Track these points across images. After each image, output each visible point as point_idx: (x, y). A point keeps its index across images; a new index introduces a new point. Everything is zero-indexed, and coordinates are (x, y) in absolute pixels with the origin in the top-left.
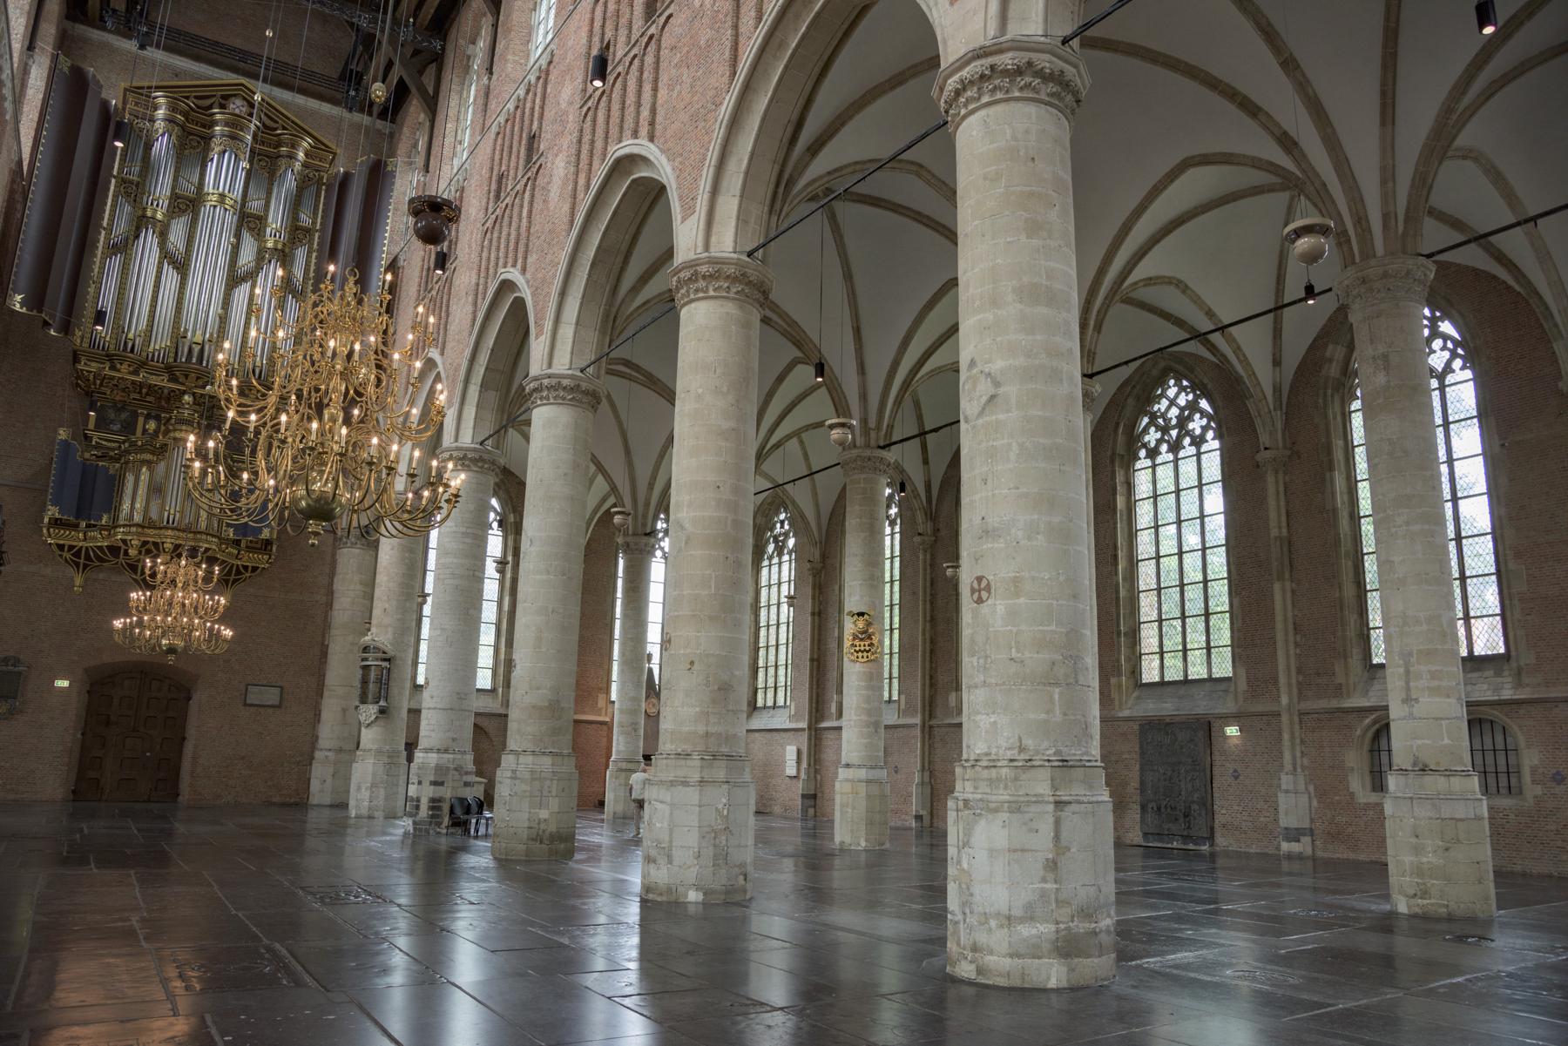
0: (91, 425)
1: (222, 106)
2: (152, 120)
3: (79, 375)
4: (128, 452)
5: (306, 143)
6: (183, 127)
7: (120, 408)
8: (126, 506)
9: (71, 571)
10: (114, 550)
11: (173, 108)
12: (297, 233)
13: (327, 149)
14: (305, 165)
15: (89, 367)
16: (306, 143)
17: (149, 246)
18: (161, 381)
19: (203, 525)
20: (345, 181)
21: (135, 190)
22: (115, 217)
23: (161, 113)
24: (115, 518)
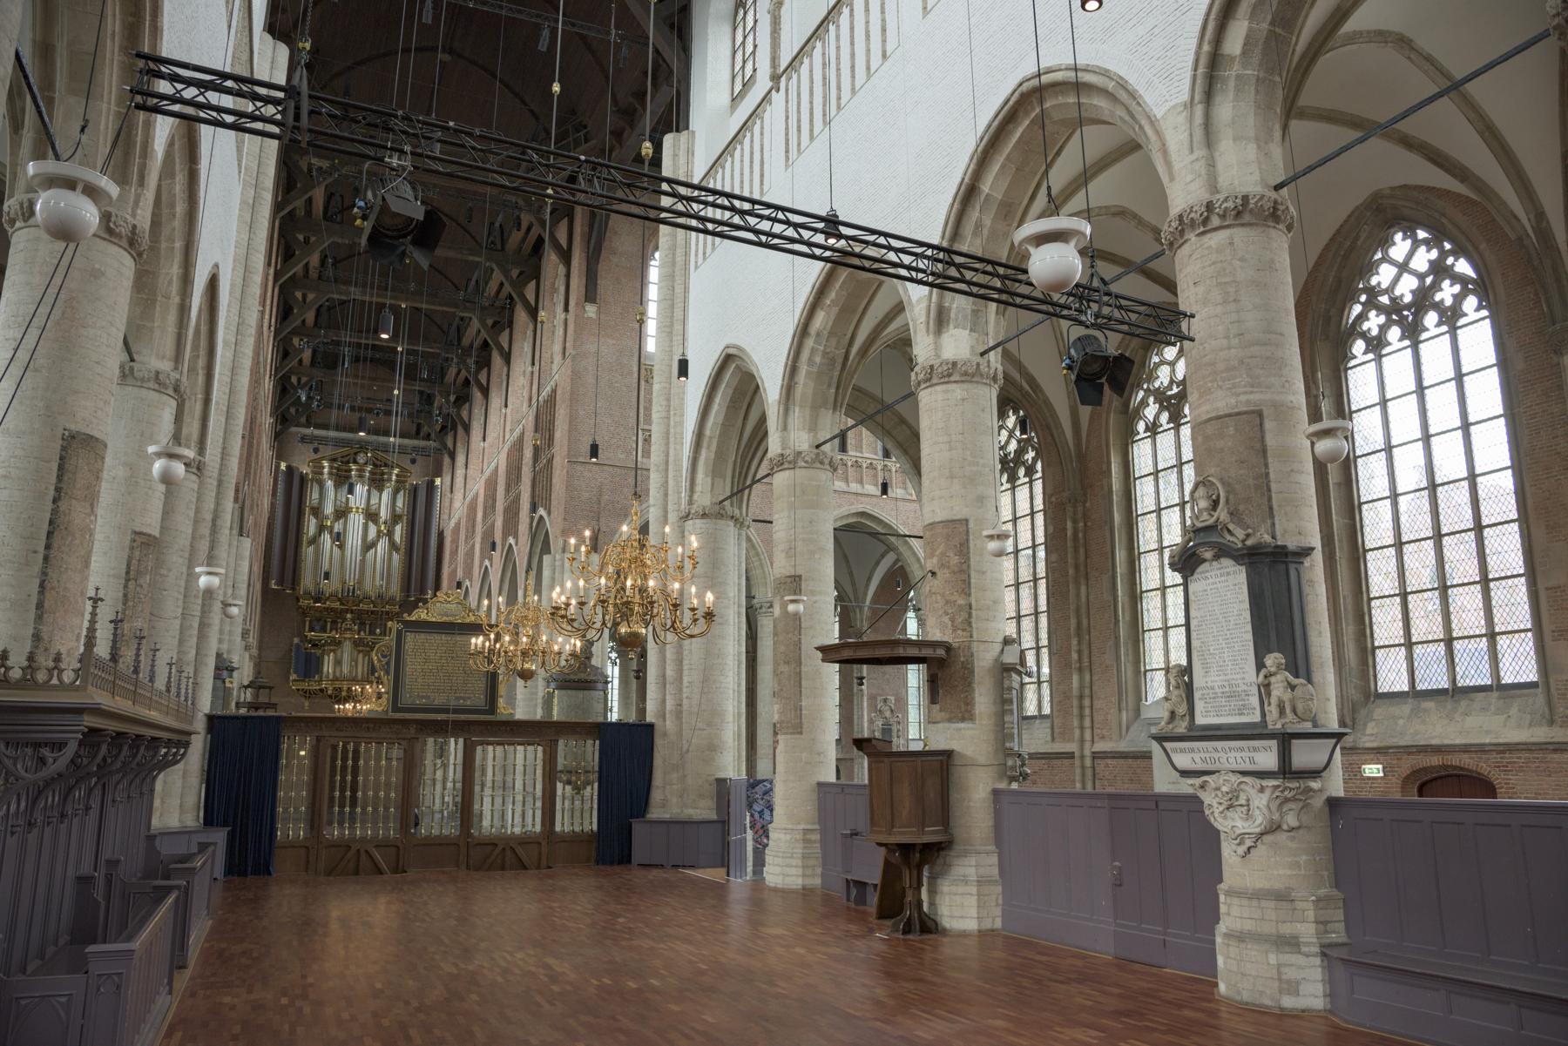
0: (307, 629)
1: (355, 462)
2: (322, 474)
3: (300, 607)
4: (324, 645)
5: (396, 471)
6: (337, 475)
7: (319, 620)
8: (325, 669)
9: (303, 699)
10: (322, 690)
11: (331, 467)
12: (396, 518)
13: (407, 471)
14: (397, 481)
15: (304, 603)
16: (396, 471)
17: (326, 538)
18: (337, 605)
19: (360, 677)
20: (415, 489)
21: (317, 511)
22: (311, 526)
23: (326, 470)
24: (321, 677)
